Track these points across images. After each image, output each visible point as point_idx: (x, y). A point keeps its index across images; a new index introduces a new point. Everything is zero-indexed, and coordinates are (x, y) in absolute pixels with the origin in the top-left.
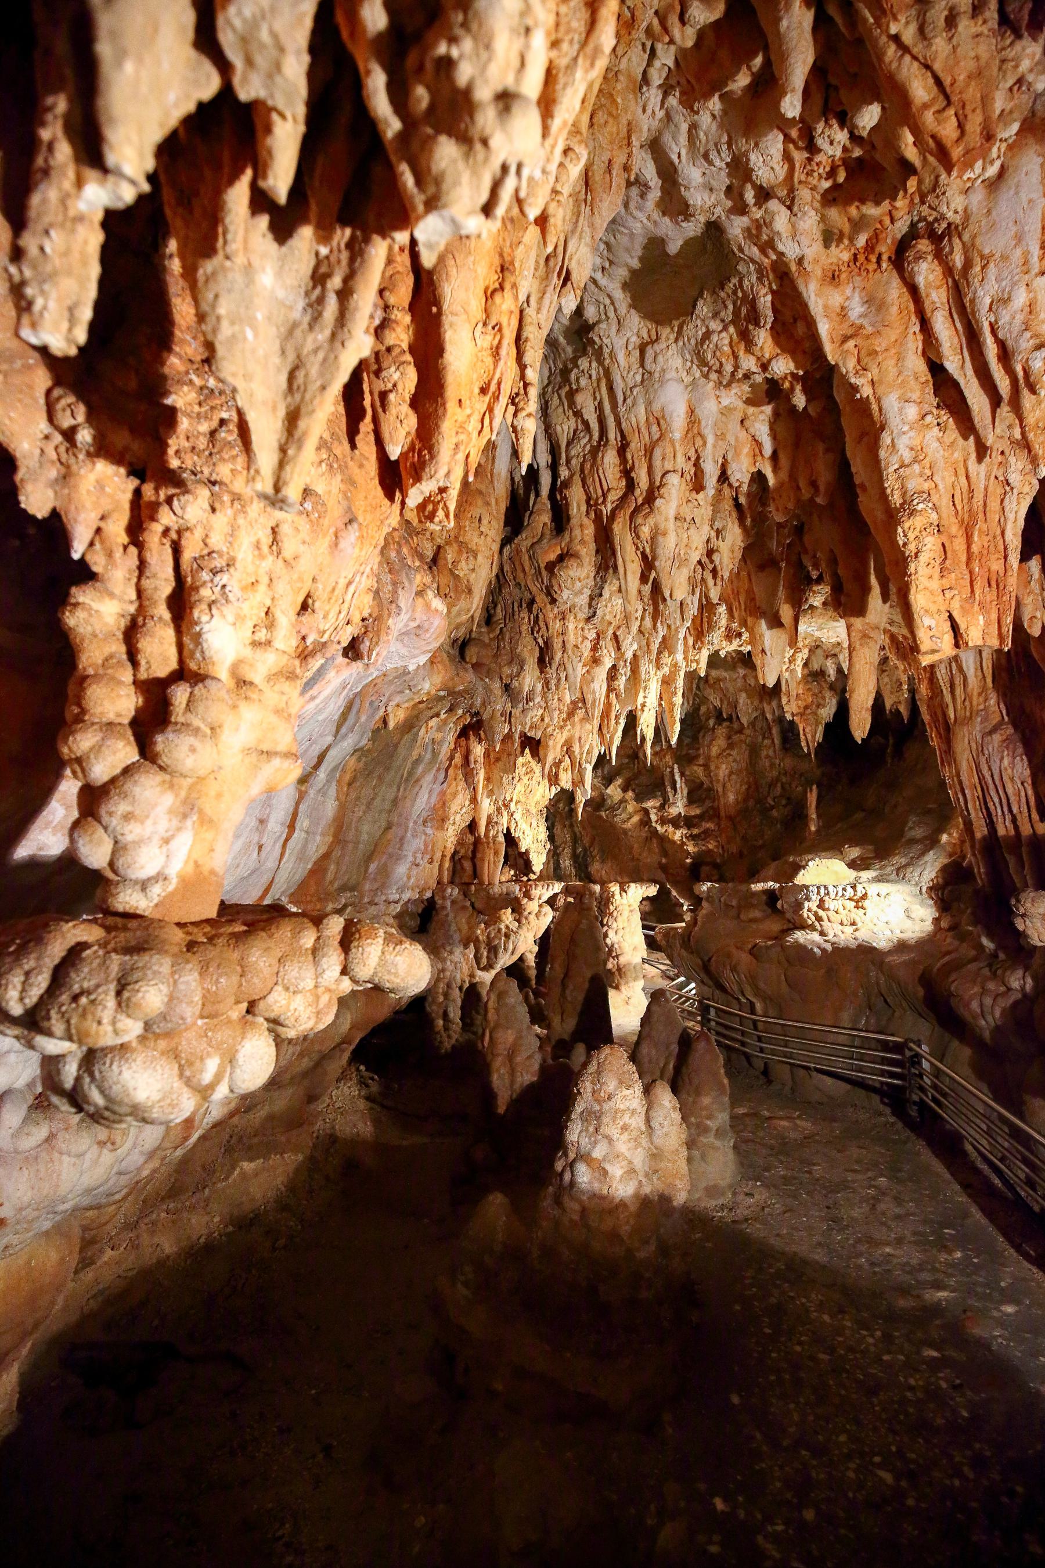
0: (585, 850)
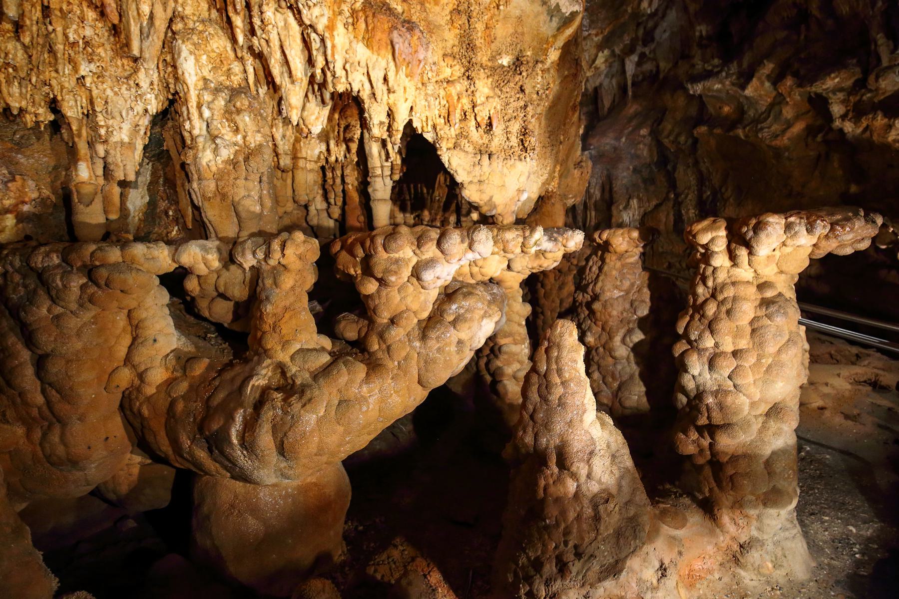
0: (715, 193)
